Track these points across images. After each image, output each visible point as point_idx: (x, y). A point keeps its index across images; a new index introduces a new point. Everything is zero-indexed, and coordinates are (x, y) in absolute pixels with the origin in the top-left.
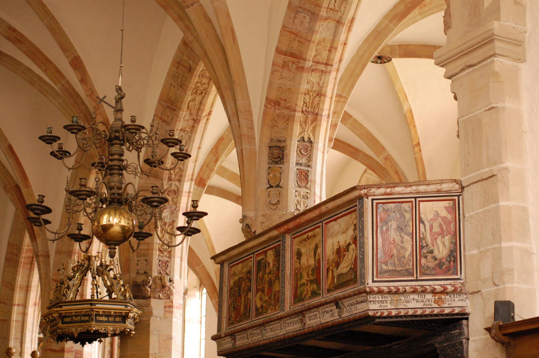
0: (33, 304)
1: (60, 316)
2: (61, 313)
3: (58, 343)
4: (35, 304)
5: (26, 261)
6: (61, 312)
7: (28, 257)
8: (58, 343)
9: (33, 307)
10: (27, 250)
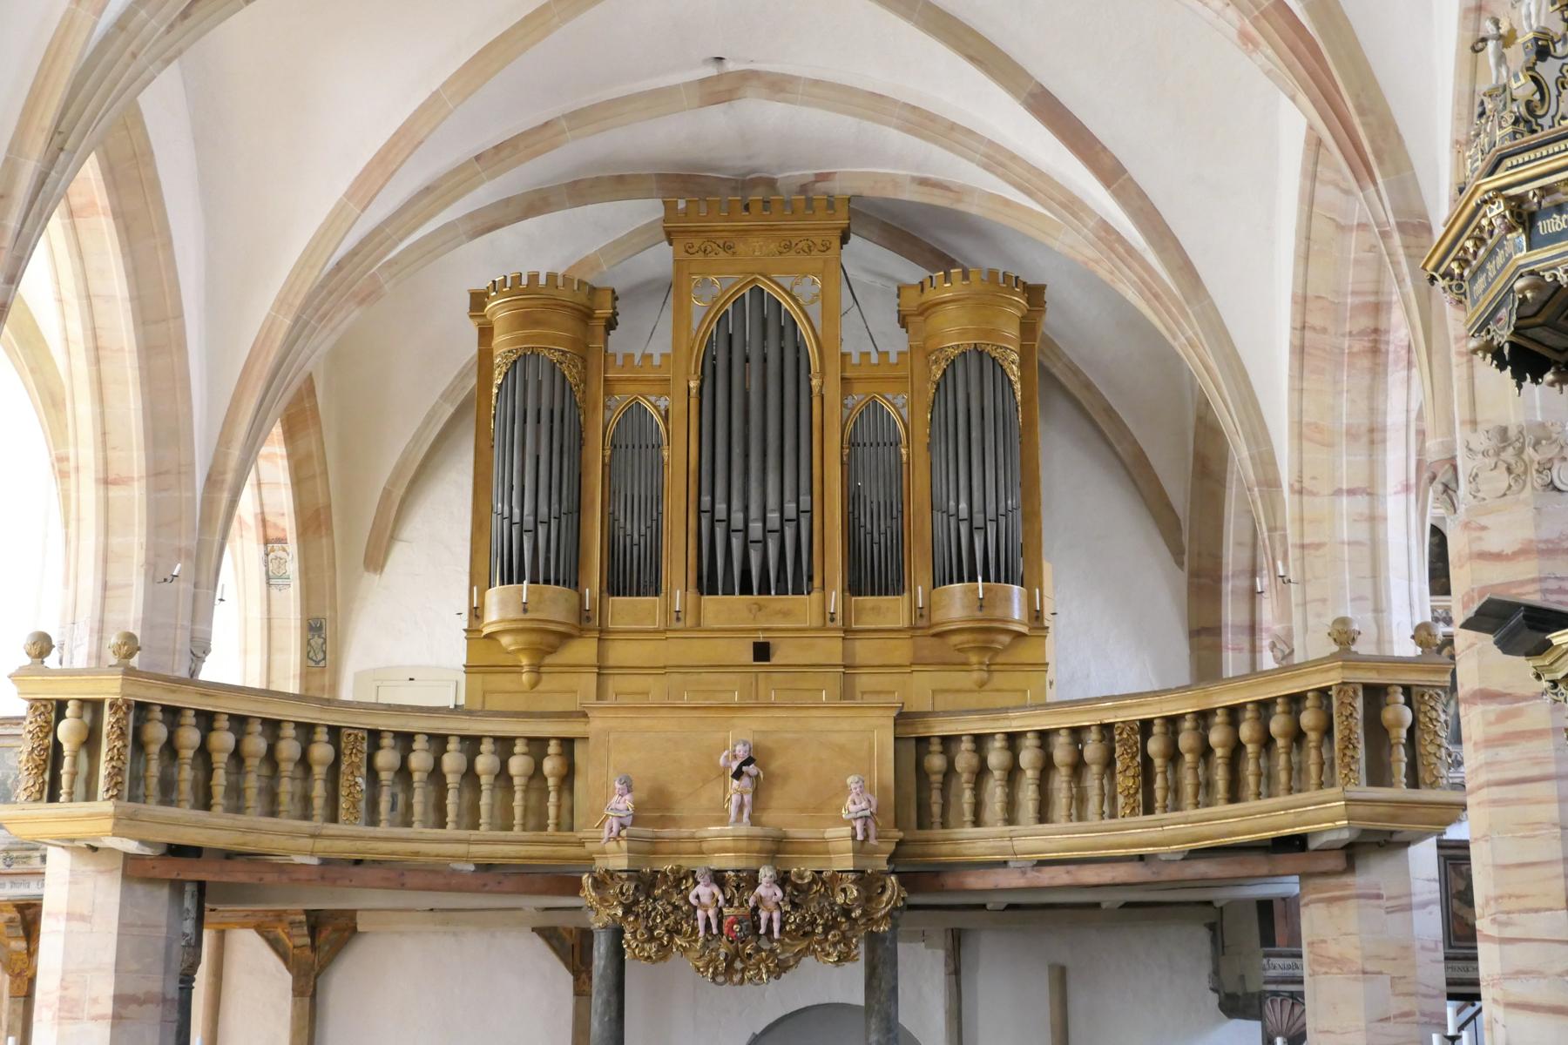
0: (1399, 488)
1: (1519, 215)
2: (1521, 199)
3: (1520, 386)
4: (1407, 488)
5: (1357, 347)
6: (1512, 192)
7: (1362, 333)
8: (1520, 386)
9: (1402, 497)
10: (1354, 308)
